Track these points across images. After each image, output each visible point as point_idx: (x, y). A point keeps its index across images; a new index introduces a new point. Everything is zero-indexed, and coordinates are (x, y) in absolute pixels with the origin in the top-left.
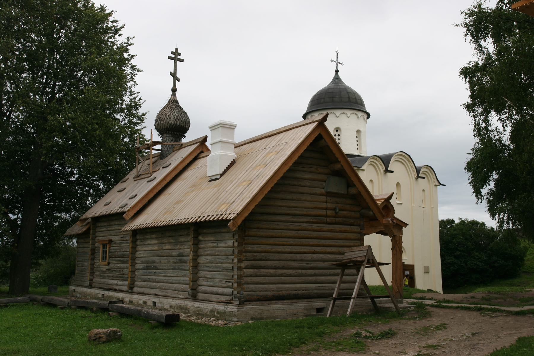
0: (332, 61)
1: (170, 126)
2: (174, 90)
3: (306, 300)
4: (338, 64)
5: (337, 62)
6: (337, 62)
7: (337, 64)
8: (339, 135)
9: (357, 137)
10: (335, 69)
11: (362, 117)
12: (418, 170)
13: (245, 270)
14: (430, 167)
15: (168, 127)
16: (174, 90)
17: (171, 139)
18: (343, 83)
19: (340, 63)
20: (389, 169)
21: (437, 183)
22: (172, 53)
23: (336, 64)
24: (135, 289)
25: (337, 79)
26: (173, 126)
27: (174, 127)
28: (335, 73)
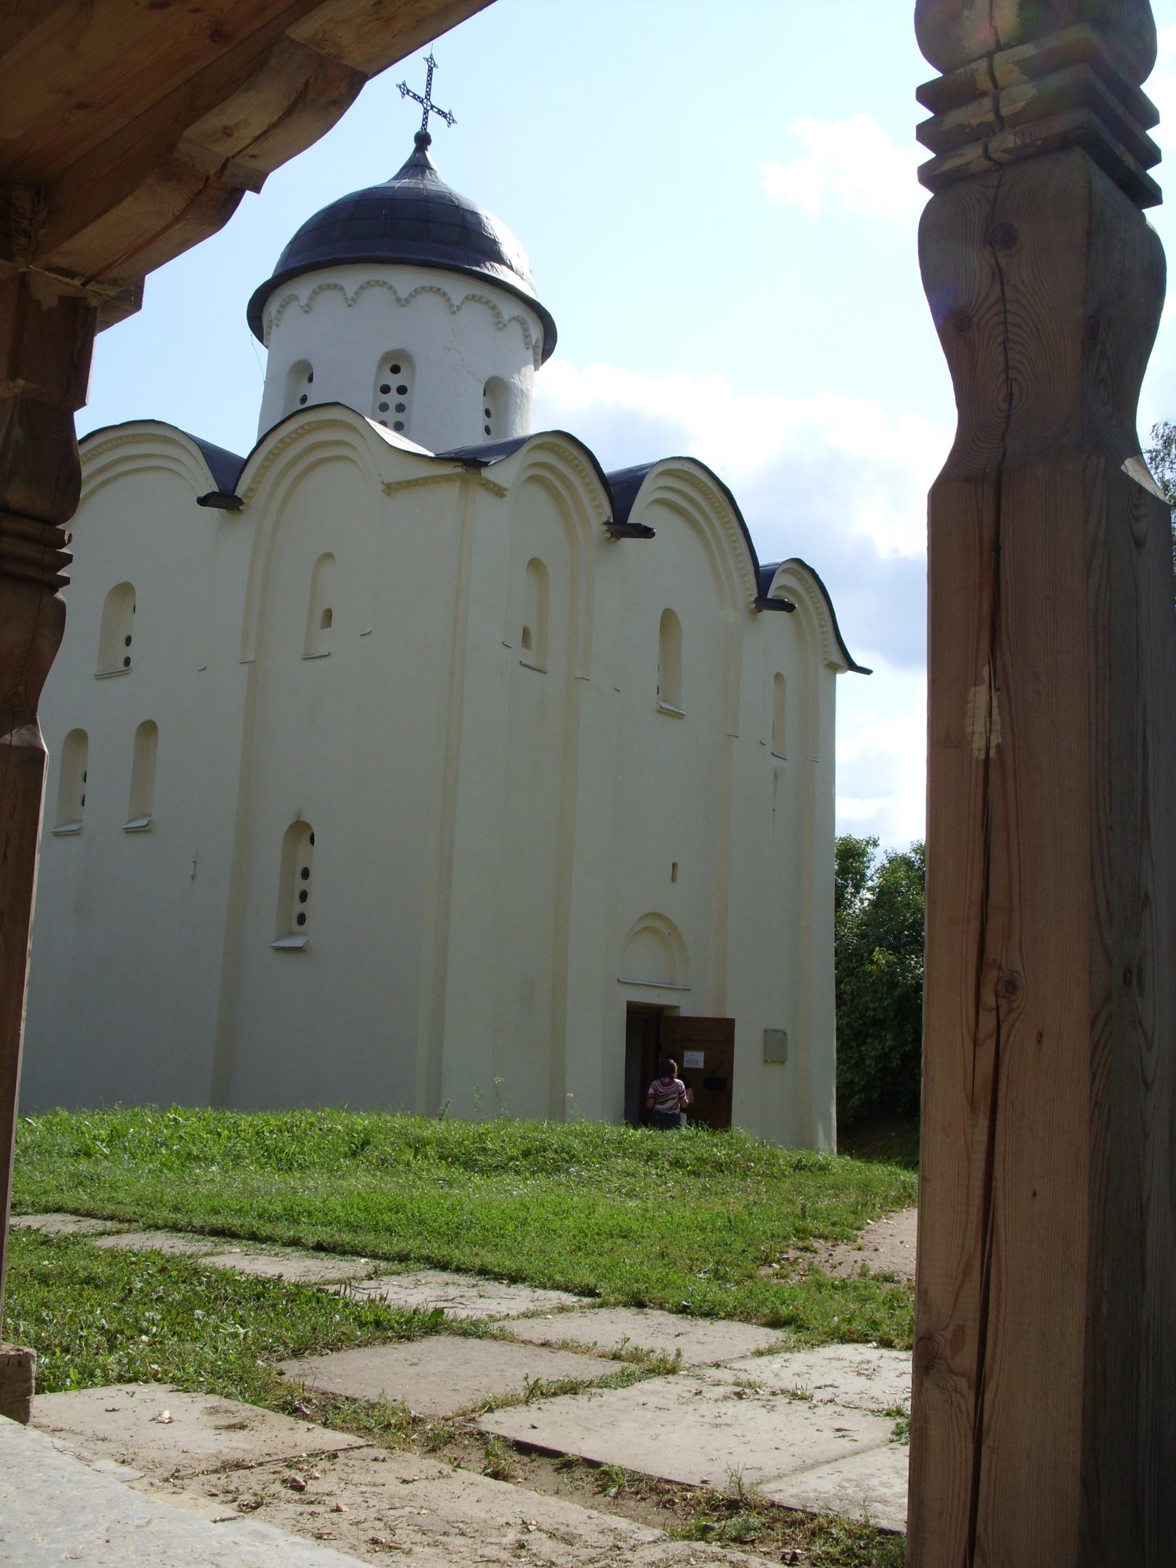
5: (424, 100)
6: (424, 100)
7: (426, 112)
8: (402, 390)
9: (488, 413)
10: (417, 128)
12: (764, 577)
14: (812, 572)
19: (441, 113)
20: (633, 519)
21: (837, 658)
23: (419, 108)
25: (418, 165)
28: (413, 146)
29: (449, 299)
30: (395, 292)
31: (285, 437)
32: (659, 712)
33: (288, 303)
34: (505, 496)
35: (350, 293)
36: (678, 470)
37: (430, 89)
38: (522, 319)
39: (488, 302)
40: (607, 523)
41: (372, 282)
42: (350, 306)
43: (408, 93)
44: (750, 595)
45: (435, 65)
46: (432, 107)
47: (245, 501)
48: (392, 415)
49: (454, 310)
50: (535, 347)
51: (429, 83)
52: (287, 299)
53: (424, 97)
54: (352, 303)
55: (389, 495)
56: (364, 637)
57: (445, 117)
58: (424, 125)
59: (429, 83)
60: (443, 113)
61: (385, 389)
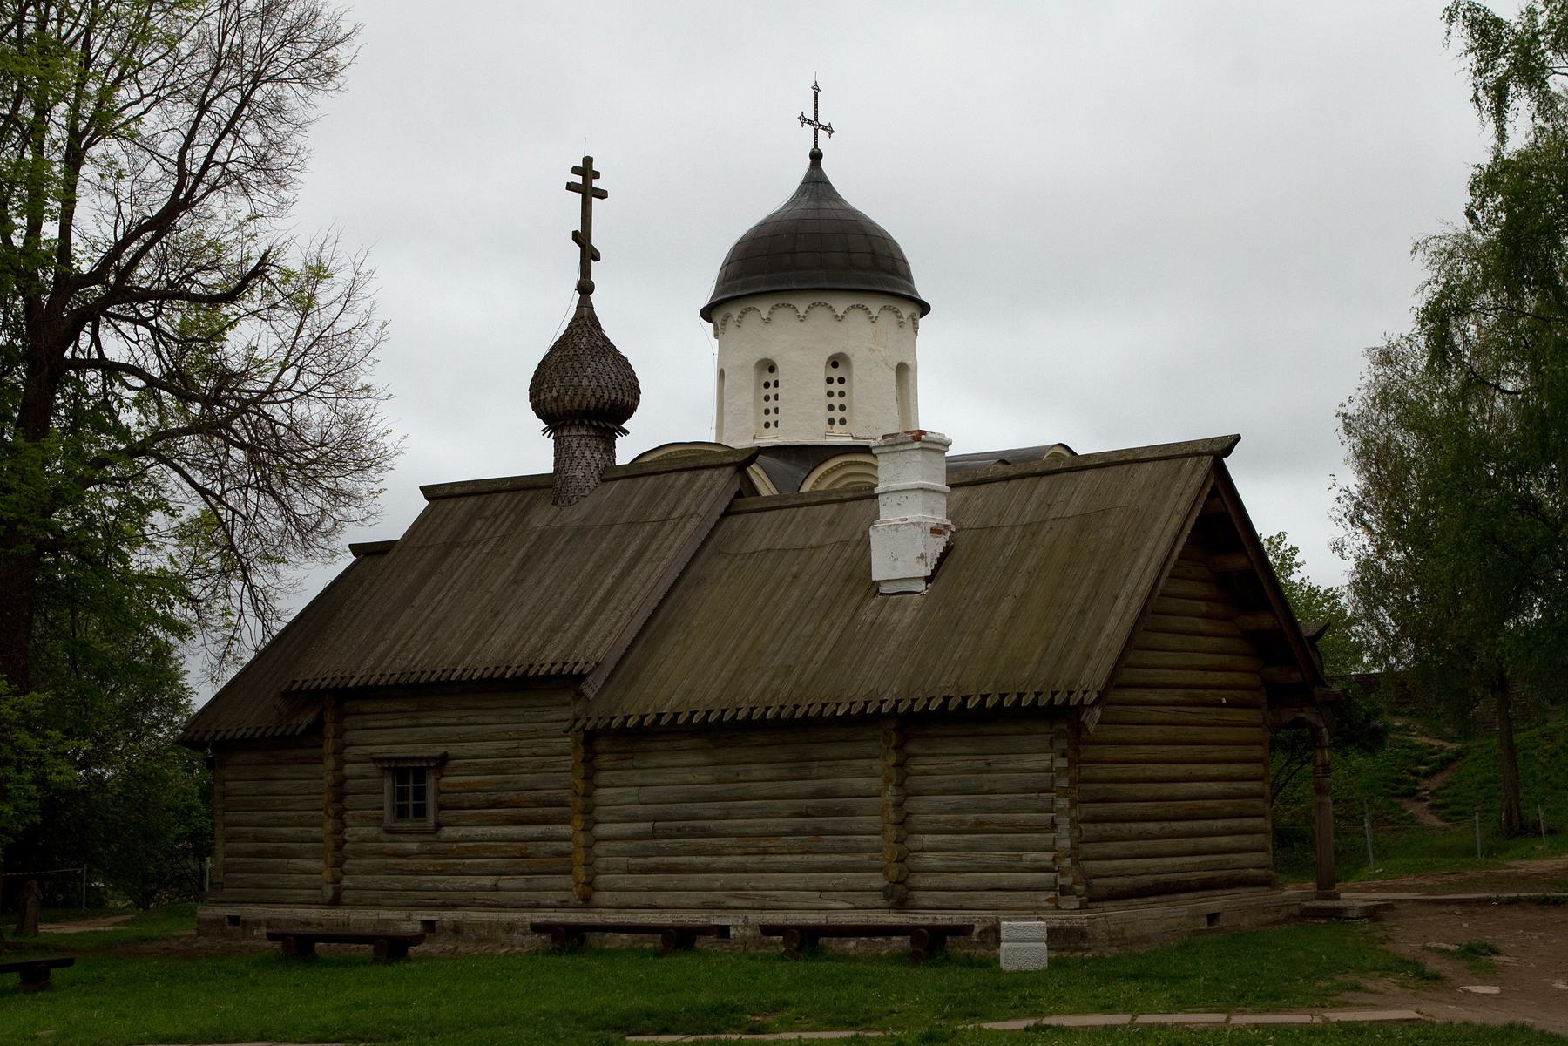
0: (803, 119)
1: (596, 405)
2: (585, 288)
3: (1182, 896)
5: (815, 123)
6: (815, 123)
8: (841, 381)
13: (1082, 826)
15: (592, 406)
16: (585, 288)
17: (592, 443)
18: (836, 197)
19: (825, 128)
22: (575, 170)
23: (810, 129)
24: (603, 897)
25: (816, 181)
26: (605, 403)
27: (607, 406)
28: (809, 161)
29: (870, 313)
35: (802, 313)
46: (820, 125)
48: (836, 401)
49: (873, 320)
58: (816, 145)
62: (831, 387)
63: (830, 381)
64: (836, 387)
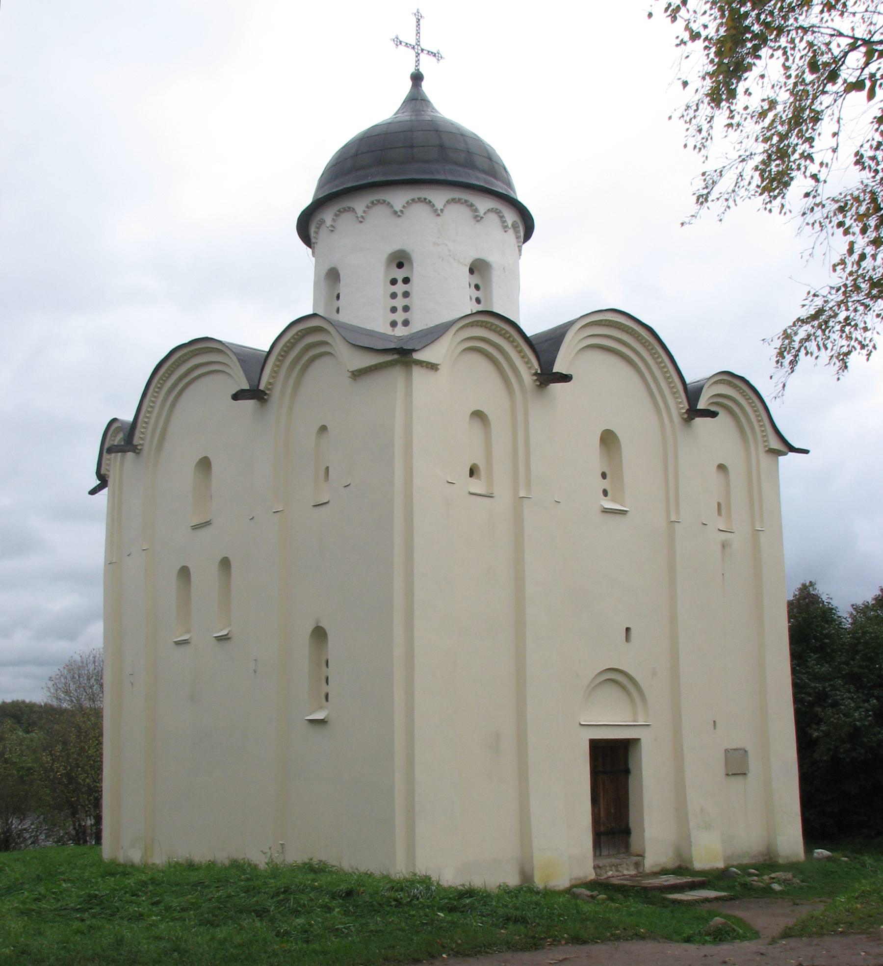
0: (398, 42)
4: (423, 57)
7: (418, 55)
11: (493, 217)
20: (558, 368)
23: (412, 53)
28: (409, 84)
29: (433, 206)
30: (392, 207)
31: (286, 343)
32: (603, 512)
33: (320, 225)
34: (439, 369)
36: (602, 320)
37: (419, 37)
38: (497, 209)
39: (466, 201)
40: (536, 374)
41: (375, 202)
42: (361, 222)
43: (401, 43)
44: (682, 408)
45: (421, 16)
46: (422, 50)
47: (267, 392)
48: (399, 302)
49: (437, 213)
50: (515, 226)
51: (418, 33)
52: (319, 222)
53: (414, 44)
54: (361, 220)
55: (355, 380)
56: (346, 488)
57: (435, 56)
59: (418, 33)
60: (432, 53)
61: (394, 282)
62: (394, 289)
63: (394, 282)
64: (400, 288)
